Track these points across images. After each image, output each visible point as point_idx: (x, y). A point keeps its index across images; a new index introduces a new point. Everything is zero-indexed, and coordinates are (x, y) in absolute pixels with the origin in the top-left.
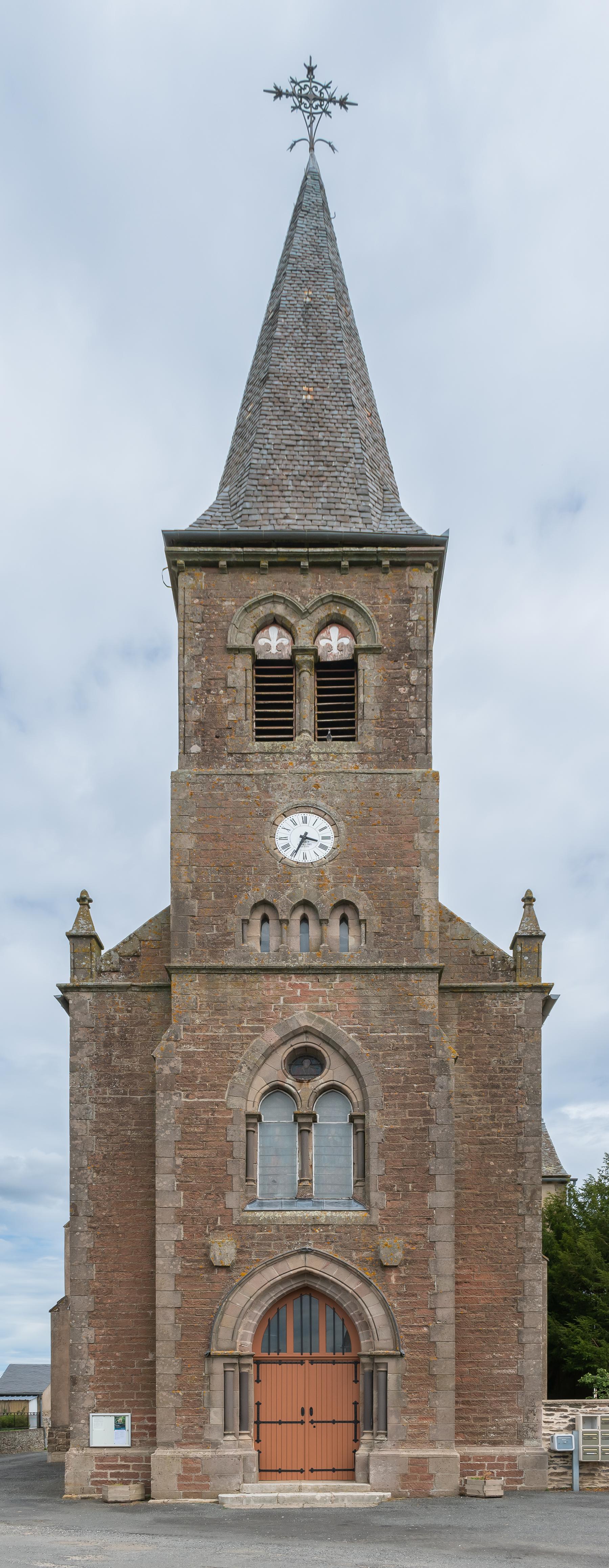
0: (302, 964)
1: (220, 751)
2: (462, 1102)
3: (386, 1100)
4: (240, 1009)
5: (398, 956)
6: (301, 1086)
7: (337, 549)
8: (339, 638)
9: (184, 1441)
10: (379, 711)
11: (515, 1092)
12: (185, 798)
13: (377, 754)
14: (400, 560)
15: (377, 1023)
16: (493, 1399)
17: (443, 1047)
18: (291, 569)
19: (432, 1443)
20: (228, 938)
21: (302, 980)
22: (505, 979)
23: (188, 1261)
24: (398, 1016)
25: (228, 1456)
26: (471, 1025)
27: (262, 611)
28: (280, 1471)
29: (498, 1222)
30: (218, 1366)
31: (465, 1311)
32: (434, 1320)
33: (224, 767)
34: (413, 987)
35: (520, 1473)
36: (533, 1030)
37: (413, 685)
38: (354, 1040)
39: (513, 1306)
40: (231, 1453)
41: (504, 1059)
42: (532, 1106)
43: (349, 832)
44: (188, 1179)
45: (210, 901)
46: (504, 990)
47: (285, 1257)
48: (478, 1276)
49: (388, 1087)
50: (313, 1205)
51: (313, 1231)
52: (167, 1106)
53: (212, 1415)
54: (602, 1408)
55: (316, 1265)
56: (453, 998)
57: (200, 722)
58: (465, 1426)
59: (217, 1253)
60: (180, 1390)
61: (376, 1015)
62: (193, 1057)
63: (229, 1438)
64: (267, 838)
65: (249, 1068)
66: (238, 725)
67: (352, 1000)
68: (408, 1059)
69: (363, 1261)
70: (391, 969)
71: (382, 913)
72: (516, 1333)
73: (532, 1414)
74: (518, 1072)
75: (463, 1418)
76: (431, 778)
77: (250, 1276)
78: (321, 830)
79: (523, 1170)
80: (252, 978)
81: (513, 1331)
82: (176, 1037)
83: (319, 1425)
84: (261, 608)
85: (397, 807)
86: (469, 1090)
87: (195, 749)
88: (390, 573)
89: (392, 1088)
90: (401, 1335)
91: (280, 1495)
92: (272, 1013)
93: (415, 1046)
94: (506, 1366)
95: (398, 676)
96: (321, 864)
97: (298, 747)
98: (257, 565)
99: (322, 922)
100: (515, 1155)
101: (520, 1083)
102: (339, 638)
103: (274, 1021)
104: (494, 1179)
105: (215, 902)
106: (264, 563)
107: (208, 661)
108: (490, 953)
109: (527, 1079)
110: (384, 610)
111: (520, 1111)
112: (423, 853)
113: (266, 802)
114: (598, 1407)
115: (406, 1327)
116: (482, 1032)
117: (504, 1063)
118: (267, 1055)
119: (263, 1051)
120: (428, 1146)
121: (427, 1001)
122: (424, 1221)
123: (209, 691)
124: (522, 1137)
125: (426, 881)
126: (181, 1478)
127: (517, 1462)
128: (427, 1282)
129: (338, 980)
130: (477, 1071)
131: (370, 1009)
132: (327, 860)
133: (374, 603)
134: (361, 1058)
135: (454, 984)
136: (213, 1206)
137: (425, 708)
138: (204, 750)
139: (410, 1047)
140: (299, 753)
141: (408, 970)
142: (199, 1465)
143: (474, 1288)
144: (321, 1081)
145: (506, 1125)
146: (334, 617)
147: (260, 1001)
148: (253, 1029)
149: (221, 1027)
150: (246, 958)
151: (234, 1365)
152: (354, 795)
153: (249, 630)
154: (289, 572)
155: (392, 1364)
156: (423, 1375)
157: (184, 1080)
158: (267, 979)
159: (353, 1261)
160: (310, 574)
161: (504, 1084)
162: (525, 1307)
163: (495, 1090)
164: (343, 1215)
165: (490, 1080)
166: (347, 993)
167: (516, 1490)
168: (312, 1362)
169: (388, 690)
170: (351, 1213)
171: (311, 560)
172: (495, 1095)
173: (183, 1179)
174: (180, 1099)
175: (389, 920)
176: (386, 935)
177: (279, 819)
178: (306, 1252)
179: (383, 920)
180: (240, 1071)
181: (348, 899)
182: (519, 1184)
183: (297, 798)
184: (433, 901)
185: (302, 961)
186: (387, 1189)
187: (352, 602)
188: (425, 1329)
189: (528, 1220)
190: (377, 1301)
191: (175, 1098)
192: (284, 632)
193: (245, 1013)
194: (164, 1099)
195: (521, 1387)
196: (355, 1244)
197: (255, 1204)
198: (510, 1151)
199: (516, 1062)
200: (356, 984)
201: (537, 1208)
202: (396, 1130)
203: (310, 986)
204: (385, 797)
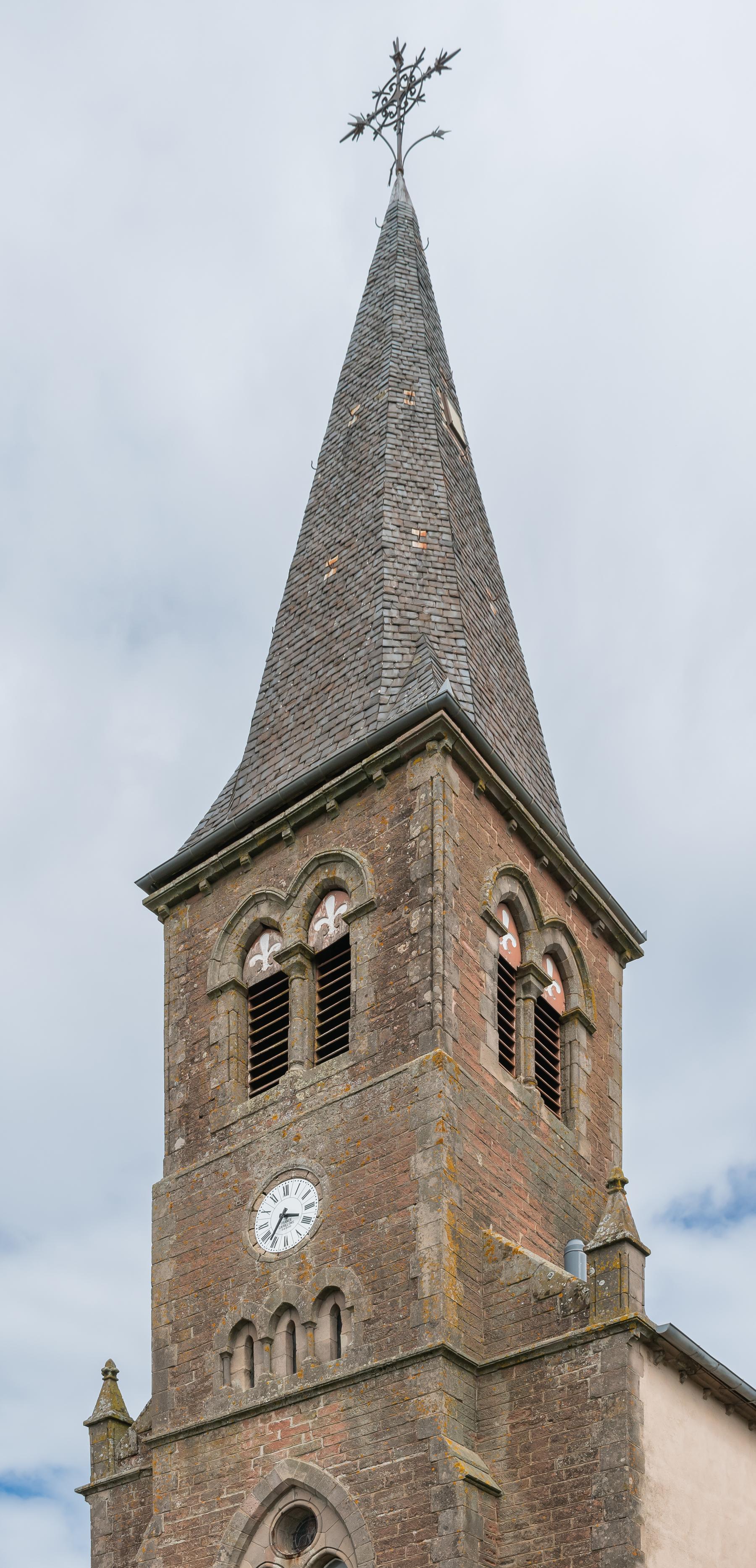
1: (203, 1133)
4: (220, 1476)
5: (392, 1348)
6: (290, 1563)
7: (316, 793)
8: (335, 910)
10: (373, 994)
12: (166, 1215)
13: (371, 1057)
14: (393, 760)
15: (367, 1453)
17: (447, 1466)
20: (206, 1384)
21: (282, 1417)
22: (579, 1324)
24: (393, 1435)
26: (528, 1413)
33: (207, 1154)
34: (411, 1386)
37: (415, 935)
38: (341, 1485)
45: (189, 1341)
49: (381, 1542)
56: (503, 1377)
61: (368, 1441)
62: (174, 1552)
64: (246, 1234)
65: (228, 1554)
67: (339, 1428)
68: (405, 1495)
70: (380, 1369)
76: (431, 1064)
78: (303, 1198)
85: (388, 1126)
87: (180, 1143)
88: (388, 783)
89: (386, 1542)
92: (252, 1472)
93: (413, 1474)
95: (397, 929)
96: (302, 1246)
97: (282, 1091)
102: (335, 910)
105: (194, 1340)
108: (558, 1289)
110: (379, 843)
112: (421, 1181)
113: (244, 1185)
116: (543, 1420)
118: (251, 1531)
119: (242, 1527)
121: (427, 1403)
125: (426, 1221)
129: (322, 1404)
131: (359, 1434)
132: (308, 1237)
133: (370, 839)
134: (349, 1508)
135: (498, 1358)
137: (429, 960)
138: (188, 1141)
139: (408, 1477)
140: (283, 1099)
141: (402, 1364)
144: (312, 1553)
146: (325, 885)
148: (233, 1500)
149: (201, 1505)
152: (339, 1131)
160: (297, 841)
166: (333, 1419)
169: (385, 958)
175: (381, 1297)
176: (378, 1320)
177: (259, 1200)
180: (219, 1560)
181: (333, 1284)
183: (275, 1164)
185: (281, 1390)
192: (275, 935)
193: (225, 1479)
200: (342, 1404)
203: (291, 1421)
204: (376, 1118)
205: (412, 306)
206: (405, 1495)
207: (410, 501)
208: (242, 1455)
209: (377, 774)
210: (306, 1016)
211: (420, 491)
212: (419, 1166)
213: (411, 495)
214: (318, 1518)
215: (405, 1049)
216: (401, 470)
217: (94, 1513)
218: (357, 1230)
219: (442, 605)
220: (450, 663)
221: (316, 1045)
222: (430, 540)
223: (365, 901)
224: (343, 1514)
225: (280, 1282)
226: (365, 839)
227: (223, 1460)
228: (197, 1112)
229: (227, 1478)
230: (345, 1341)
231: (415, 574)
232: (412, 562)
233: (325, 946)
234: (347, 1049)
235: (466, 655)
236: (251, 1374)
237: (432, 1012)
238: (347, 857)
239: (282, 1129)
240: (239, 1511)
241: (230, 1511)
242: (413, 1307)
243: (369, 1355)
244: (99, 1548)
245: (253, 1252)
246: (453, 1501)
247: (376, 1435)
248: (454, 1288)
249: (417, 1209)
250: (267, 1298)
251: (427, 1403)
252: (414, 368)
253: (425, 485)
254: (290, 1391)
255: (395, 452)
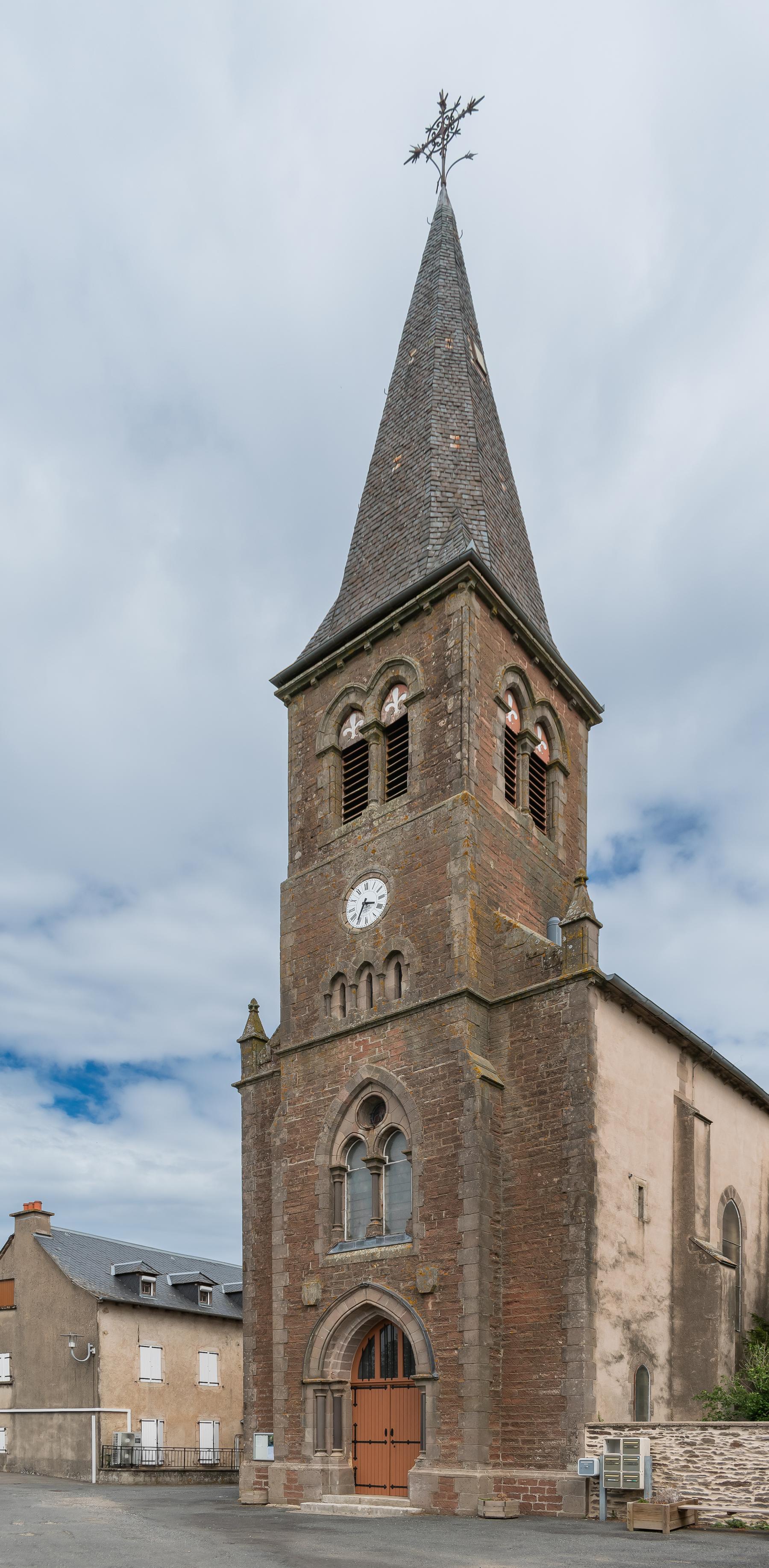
0: (365, 1021)
1: (313, 848)
2: (513, 1116)
3: (425, 1133)
4: (324, 1076)
5: (434, 991)
9: (290, 1456)
11: (561, 1094)
13: (421, 797)
14: (437, 595)
16: (540, 1421)
17: (469, 1069)
18: (361, 655)
19: (460, 1463)
23: (292, 1303)
25: (314, 1470)
27: (340, 707)
28: (370, 1486)
29: (544, 1235)
30: (310, 1392)
31: (515, 1331)
32: (462, 1343)
33: (316, 862)
35: (560, 1498)
36: (577, 1023)
37: (450, 714)
38: (401, 1081)
39: (558, 1323)
40: (317, 1467)
41: (551, 1062)
42: (576, 1106)
43: (397, 882)
44: (292, 1233)
45: (304, 987)
46: (549, 988)
47: (352, 1293)
48: (526, 1294)
49: (427, 1120)
50: (377, 1242)
51: (372, 1266)
52: (279, 1173)
53: (307, 1434)
54: (645, 1431)
55: (373, 1298)
57: (301, 830)
58: (514, 1448)
59: (306, 1294)
60: (287, 1413)
61: (418, 1053)
62: (294, 1126)
63: (318, 1454)
64: (341, 916)
66: (325, 820)
67: (399, 1044)
68: (442, 1089)
69: (408, 1290)
70: (427, 1005)
71: (422, 952)
72: (560, 1351)
73: (574, 1437)
74: (564, 1072)
75: (512, 1440)
76: (460, 801)
77: (329, 1312)
79: (567, 1177)
80: (330, 1046)
81: (558, 1349)
82: (284, 1112)
83: (398, 1444)
84: (339, 705)
86: (520, 1102)
87: (298, 855)
89: (430, 1120)
90: (437, 1360)
91: (335, 1505)
94: (551, 1386)
98: (335, 668)
99: (382, 976)
100: (560, 1162)
101: (565, 1083)
103: (346, 1080)
104: (541, 1191)
105: (307, 986)
106: (340, 663)
107: (306, 773)
109: (572, 1078)
110: (428, 652)
111: (564, 1114)
112: (453, 880)
113: (339, 883)
114: (642, 1430)
115: (440, 1350)
117: (551, 1066)
118: (344, 1112)
120: (457, 1172)
121: (456, 1028)
122: (455, 1246)
123: (306, 800)
124: (567, 1142)
125: (457, 906)
126: (286, 1487)
127: (556, 1487)
128: (457, 1306)
129: (389, 1028)
130: (527, 1081)
132: (380, 918)
133: (421, 649)
134: (406, 1097)
135: (503, 997)
136: (307, 1253)
137: (459, 731)
138: (304, 854)
139: (444, 1077)
140: (364, 825)
141: (440, 1002)
142: (296, 1477)
143: (523, 1306)
144: (382, 1126)
145: (553, 1132)
146: (392, 681)
148: (332, 1092)
149: (312, 1095)
150: (326, 1030)
151: (322, 1391)
152: (401, 847)
153: (332, 730)
154: (358, 659)
155: (429, 1388)
156: (454, 1397)
157: (290, 1148)
158: (341, 1043)
159: (400, 1292)
161: (550, 1089)
162: (569, 1323)
163: (542, 1097)
164: (393, 1249)
165: (538, 1087)
167: (555, 1516)
168: (393, 1387)
170: (400, 1246)
171: (371, 640)
172: (542, 1102)
173: (288, 1233)
174: (286, 1164)
175: (427, 957)
176: (425, 972)
177: (349, 893)
178: (366, 1286)
179: (423, 959)
181: (396, 949)
182: (564, 1193)
184: (462, 925)
186: (425, 1219)
187: (401, 660)
188: (456, 1352)
189: (572, 1230)
190: (417, 1328)
191: (283, 1165)
192: (360, 715)
193: (327, 1078)
194: (277, 1167)
195: (564, 1408)
196: (402, 1275)
197: (337, 1247)
198: (555, 1159)
199: (562, 1061)
200: (402, 1028)
201: (581, 1216)
202: (434, 1159)
205: (451, 278)
206: (442, 1089)
207: (449, 416)
208: (338, 1062)
209: (426, 605)
210: (380, 769)
211: (456, 408)
212: (452, 870)
213: (450, 411)
214: (386, 1104)
215: (443, 791)
216: (443, 394)
217: (244, 1100)
218: (412, 913)
219: (470, 487)
220: (475, 527)
221: (386, 788)
222: (462, 442)
223: (418, 691)
224: (402, 1101)
225: (362, 948)
226: (418, 650)
228: (309, 834)
230: (404, 986)
231: (452, 466)
232: (450, 458)
233: (392, 722)
234: (406, 791)
235: (485, 521)
236: (343, 1008)
237: (461, 766)
238: (406, 662)
239: (364, 846)
240: (336, 1099)
241: (330, 1099)
242: (448, 964)
243: (420, 996)
244: (247, 1123)
245: (345, 928)
246: (473, 1092)
247: (424, 1049)
248: (475, 951)
249: (451, 898)
250: (354, 958)
251: (456, 1028)
252: (452, 323)
253: (459, 404)
254: (369, 1020)
255: (439, 382)
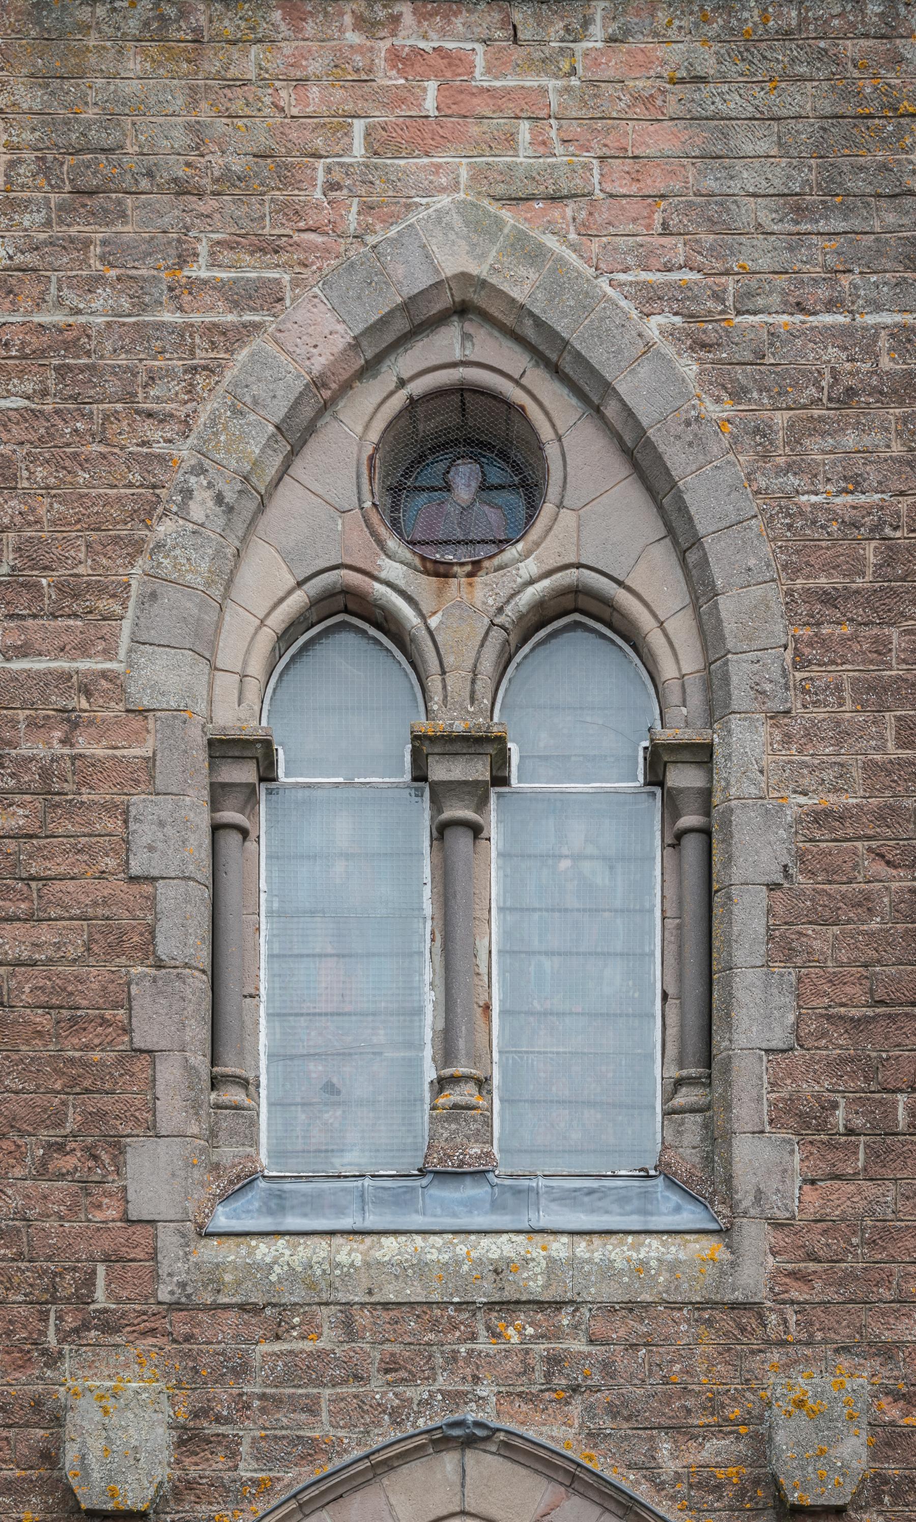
21: (443, 34)
65: (219, 499)
92: (318, 207)
119: (279, 410)
129: (597, 30)
131: (735, 186)
147: (263, 141)
180: (183, 513)
203: (480, 61)
227: (195, 129)
229: (209, 204)
